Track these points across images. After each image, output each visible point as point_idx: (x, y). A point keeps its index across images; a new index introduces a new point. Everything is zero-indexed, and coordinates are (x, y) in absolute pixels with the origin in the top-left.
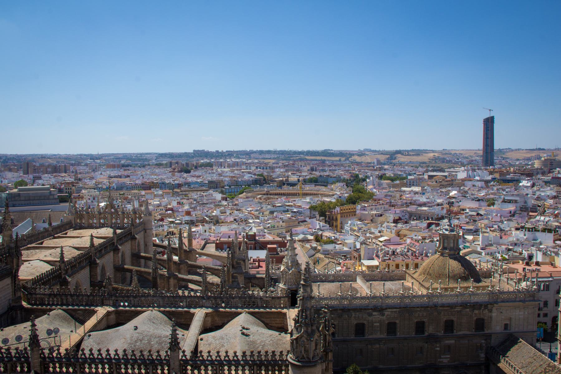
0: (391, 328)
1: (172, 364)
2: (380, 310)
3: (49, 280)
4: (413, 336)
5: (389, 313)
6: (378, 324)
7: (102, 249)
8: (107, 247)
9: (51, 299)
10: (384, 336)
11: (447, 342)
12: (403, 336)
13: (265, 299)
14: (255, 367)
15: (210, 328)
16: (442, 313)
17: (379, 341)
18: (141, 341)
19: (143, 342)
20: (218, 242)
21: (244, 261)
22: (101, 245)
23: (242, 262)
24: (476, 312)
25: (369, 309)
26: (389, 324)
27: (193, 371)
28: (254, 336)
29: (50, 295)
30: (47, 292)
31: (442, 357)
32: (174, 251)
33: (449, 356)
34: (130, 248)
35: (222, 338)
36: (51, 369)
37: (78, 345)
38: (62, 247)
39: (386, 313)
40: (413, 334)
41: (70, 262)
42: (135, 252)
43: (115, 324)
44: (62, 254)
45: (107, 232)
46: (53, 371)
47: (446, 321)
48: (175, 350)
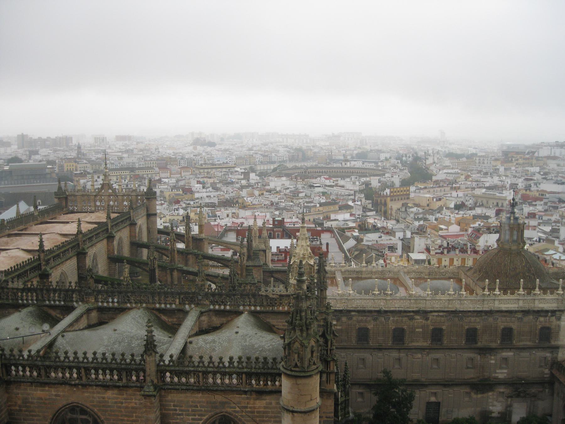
1: (148, 370)
2: (425, 313)
3: (26, 272)
6: (421, 330)
7: (93, 237)
8: (99, 233)
9: (24, 294)
11: (505, 354)
13: (271, 296)
15: (206, 330)
16: (499, 320)
18: (120, 343)
19: (123, 344)
20: (239, 228)
21: (264, 251)
22: (91, 231)
23: (262, 253)
24: (542, 319)
25: (410, 312)
26: (434, 330)
27: (173, 379)
28: (251, 339)
29: (23, 290)
30: (21, 286)
31: (497, 371)
32: (180, 237)
33: (506, 371)
34: (128, 236)
35: (214, 341)
36: (14, 373)
37: (51, 345)
38: (41, 235)
39: (430, 316)
41: (51, 251)
42: (134, 240)
43: (97, 324)
44: (41, 242)
45: (101, 217)
46: (16, 375)
48: (151, 354)
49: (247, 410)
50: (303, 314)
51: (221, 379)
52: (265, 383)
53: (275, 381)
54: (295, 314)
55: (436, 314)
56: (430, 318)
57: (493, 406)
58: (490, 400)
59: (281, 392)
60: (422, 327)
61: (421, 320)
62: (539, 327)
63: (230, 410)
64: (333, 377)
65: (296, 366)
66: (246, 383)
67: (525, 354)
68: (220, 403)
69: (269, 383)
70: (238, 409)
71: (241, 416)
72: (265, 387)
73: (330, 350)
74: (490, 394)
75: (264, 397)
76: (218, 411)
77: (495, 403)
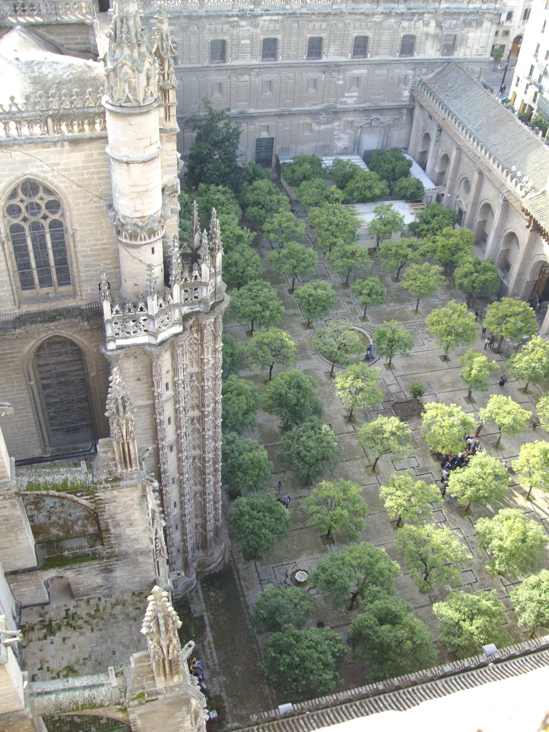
0: (270, 48)
4: (302, 61)
5: (267, 23)
6: (248, 42)
10: (257, 61)
11: (355, 72)
12: (288, 61)
14: (50, 121)
17: (248, 69)
24: (405, 24)
26: (266, 41)
33: (356, 94)
40: (304, 59)
47: (357, 39)
49: (60, 167)
50: (131, 23)
51: (17, 129)
52: (81, 127)
53: (94, 123)
54: (119, 24)
55: (268, 18)
56: (261, 24)
57: (339, 139)
58: (335, 133)
59: (106, 138)
60: (251, 37)
61: (248, 28)
62: (402, 34)
63: (34, 171)
64: (173, 111)
65: (128, 100)
66: (54, 131)
67: (382, 71)
68: (20, 162)
69: (86, 127)
70: (46, 168)
71: (52, 176)
72: (81, 134)
73: (168, 75)
74: (336, 124)
75: (80, 147)
76: (19, 173)
77: (342, 135)
